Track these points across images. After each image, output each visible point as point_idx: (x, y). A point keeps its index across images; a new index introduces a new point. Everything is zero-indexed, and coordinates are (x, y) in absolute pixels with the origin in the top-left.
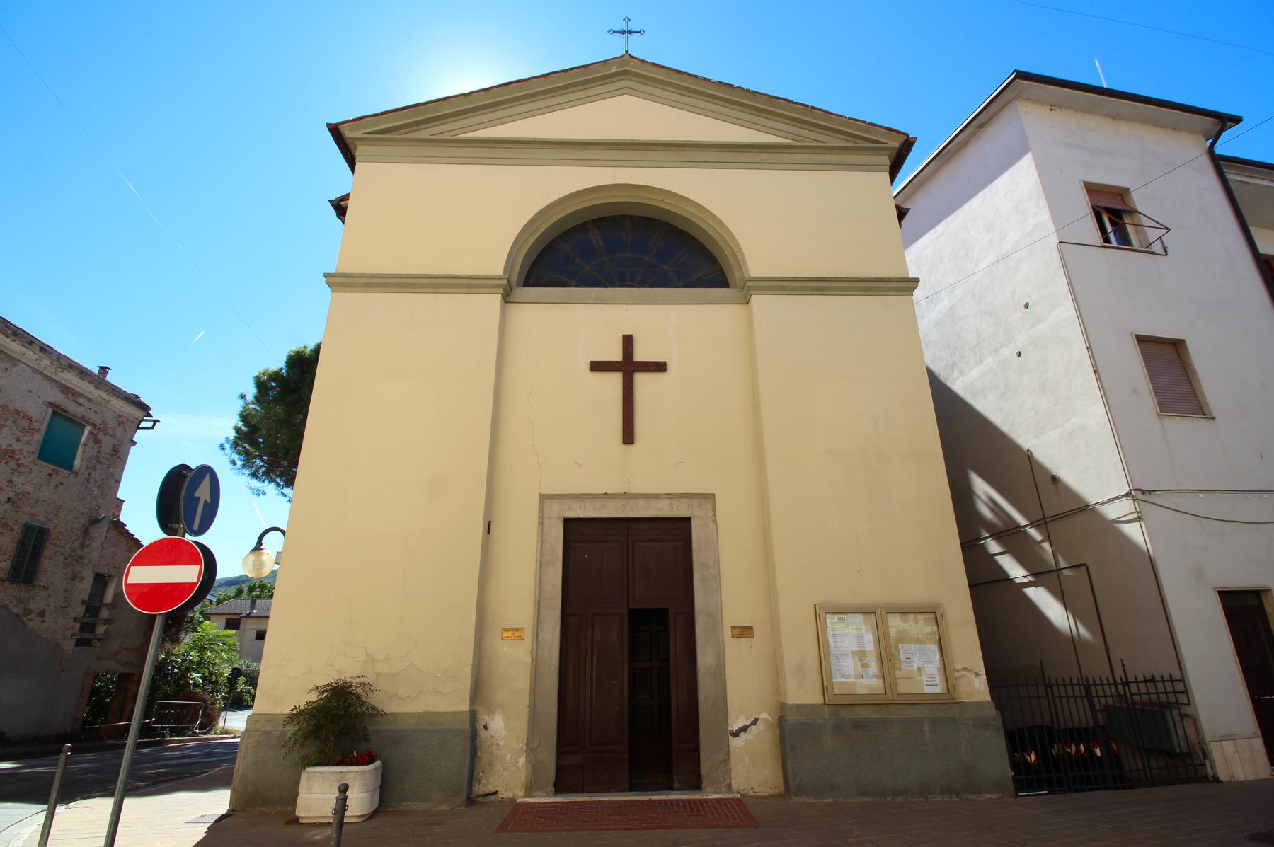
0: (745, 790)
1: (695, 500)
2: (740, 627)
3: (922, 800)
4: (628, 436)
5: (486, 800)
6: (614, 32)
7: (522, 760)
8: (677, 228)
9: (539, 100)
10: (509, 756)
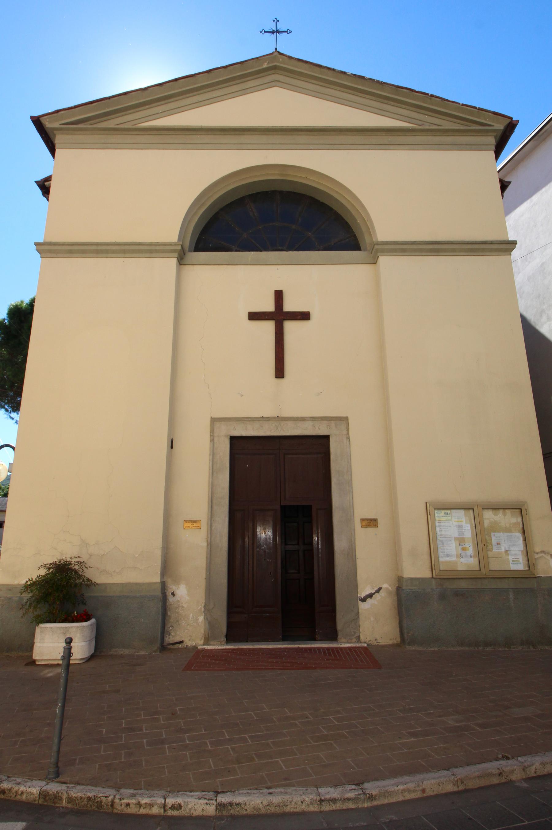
0: (370, 641)
1: (332, 422)
2: (367, 520)
3: (506, 649)
4: (280, 372)
7: (201, 618)
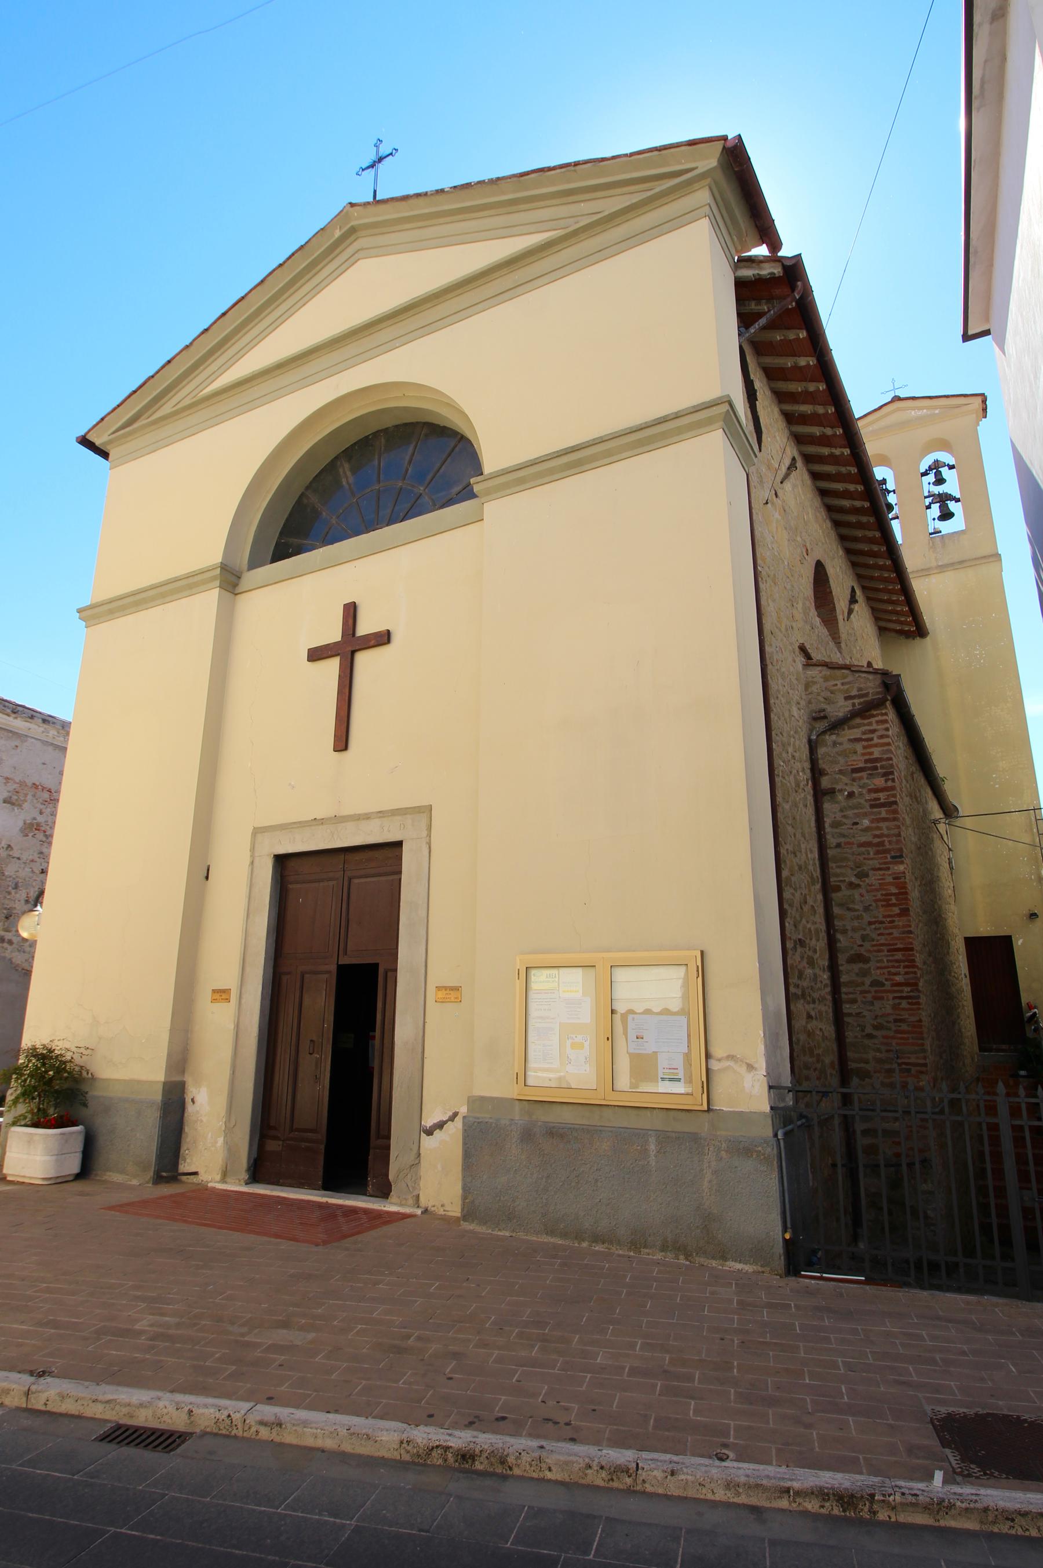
0: (434, 1206)
1: (408, 816)
2: (446, 988)
3: (632, 1254)
4: (342, 742)
5: (190, 1181)
6: (363, 170)
7: (220, 1141)
8: (438, 426)
9: (266, 316)
10: (210, 1134)
